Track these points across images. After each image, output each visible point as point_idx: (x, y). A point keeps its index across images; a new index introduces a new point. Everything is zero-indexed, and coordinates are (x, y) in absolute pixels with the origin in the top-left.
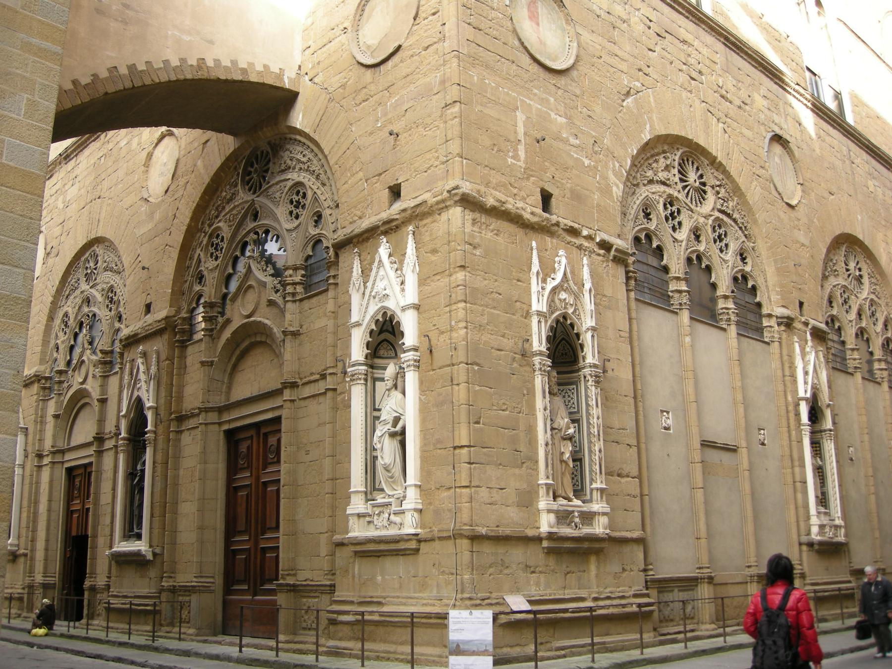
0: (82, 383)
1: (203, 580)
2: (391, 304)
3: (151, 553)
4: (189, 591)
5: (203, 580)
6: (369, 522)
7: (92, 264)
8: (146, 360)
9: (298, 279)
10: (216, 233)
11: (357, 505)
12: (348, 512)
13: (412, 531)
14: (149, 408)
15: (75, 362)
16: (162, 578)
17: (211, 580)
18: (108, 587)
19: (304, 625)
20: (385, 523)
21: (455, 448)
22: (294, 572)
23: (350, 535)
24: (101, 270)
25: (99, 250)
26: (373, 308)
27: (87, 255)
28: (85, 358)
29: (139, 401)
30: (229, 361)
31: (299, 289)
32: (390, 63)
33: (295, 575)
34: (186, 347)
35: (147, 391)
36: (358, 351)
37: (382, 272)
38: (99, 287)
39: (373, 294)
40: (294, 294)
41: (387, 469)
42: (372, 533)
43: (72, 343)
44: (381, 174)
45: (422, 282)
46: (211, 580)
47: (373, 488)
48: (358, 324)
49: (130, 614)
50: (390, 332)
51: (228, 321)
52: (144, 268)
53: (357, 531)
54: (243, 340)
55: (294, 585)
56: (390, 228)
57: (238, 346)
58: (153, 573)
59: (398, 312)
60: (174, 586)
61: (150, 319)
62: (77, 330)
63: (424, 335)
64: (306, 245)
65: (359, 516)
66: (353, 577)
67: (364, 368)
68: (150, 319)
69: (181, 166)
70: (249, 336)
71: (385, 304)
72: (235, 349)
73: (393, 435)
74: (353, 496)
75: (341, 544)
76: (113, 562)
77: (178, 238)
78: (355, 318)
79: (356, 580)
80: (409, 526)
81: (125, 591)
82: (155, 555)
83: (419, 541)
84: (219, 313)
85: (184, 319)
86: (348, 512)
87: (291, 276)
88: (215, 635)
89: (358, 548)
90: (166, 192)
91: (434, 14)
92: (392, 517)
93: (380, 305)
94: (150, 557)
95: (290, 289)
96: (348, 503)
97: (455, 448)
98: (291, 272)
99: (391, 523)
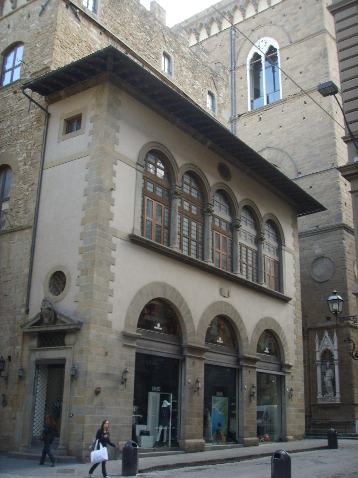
2: (329, 348)
11: (320, 396)
13: (339, 403)
20: (330, 400)
21: (350, 384)
23: (318, 403)
26: (323, 348)
32: (325, 283)
36: (318, 358)
37: (326, 340)
39: (324, 344)
41: (329, 387)
42: (325, 403)
44: (324, 313)
45: (339, 343)
47: (324, 392)
53: (320, 402)
56: (328, 328)
59: (333, 351)
63: (339, 356)
65: (321, 398)
67: (320, 362)
71: (328, 347)
73: (330, 380)
75: (314, 405)
78: (317, 350)
80: (338, 401)
91: (339, 274)
93: (325, 348)
96: (317, 395)
97: (350, 384)
99: (331, 400)
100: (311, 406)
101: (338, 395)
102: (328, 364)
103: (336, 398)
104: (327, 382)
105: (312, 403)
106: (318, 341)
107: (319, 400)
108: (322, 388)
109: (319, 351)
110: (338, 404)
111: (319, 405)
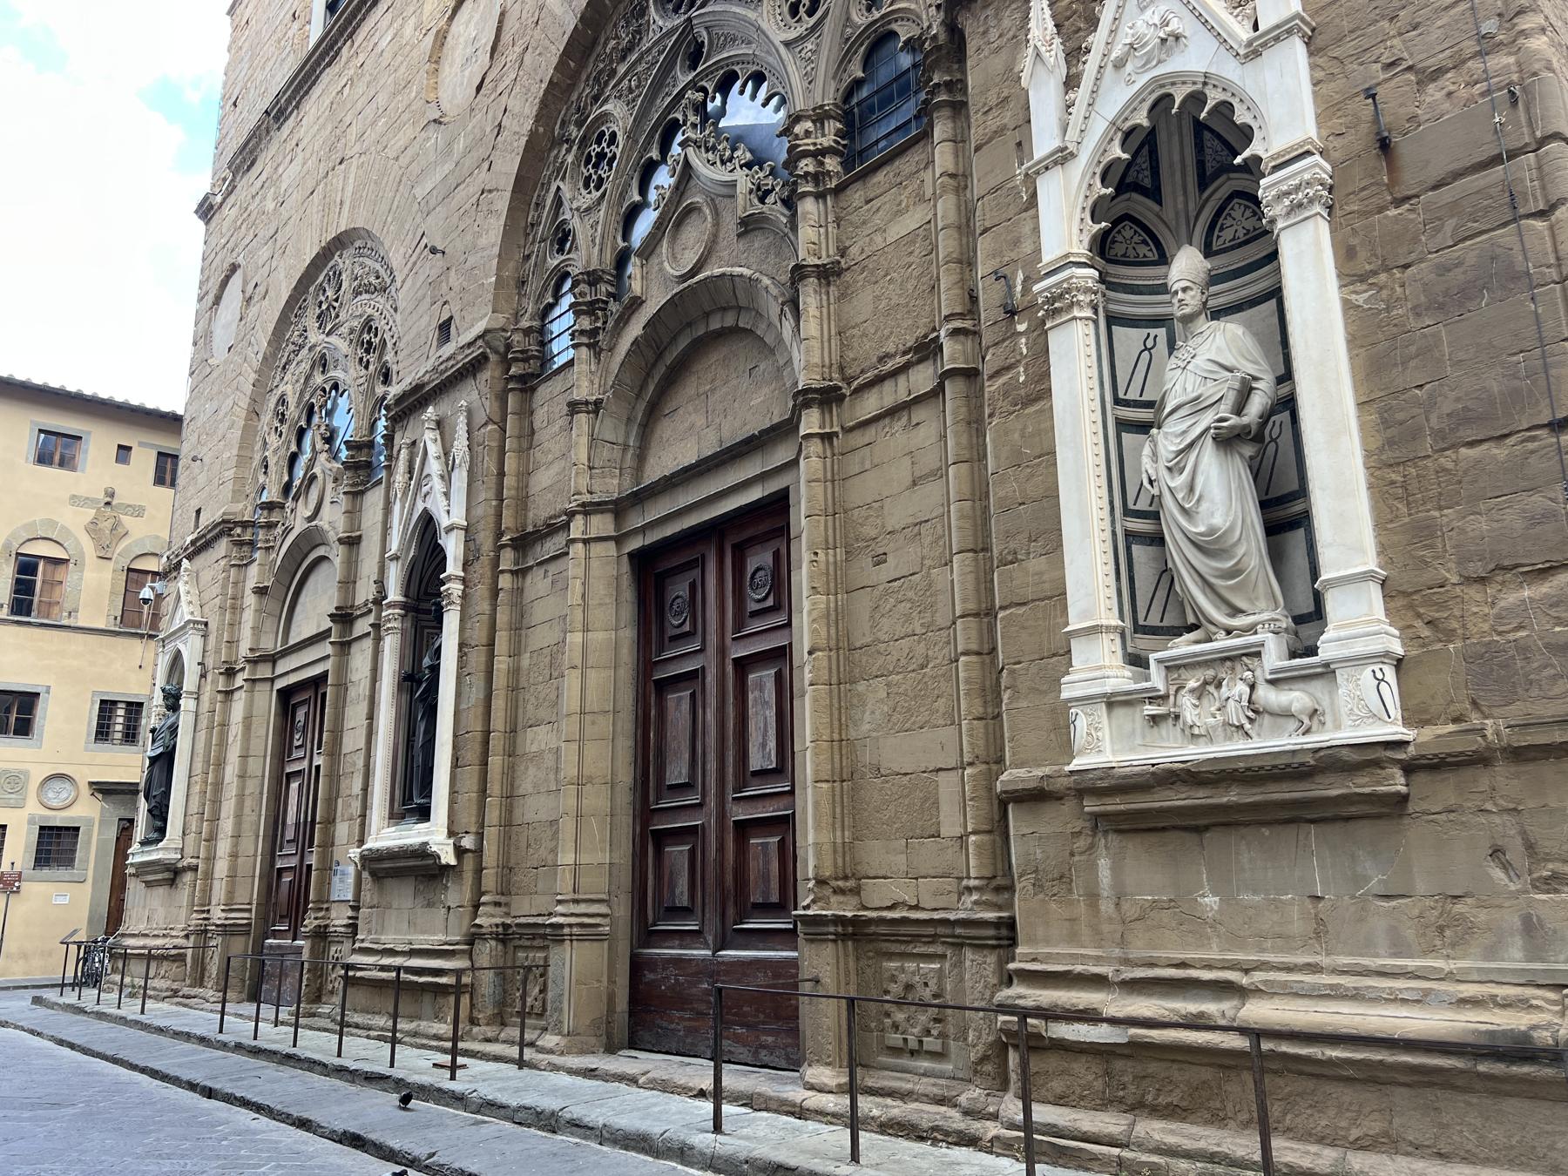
0: (310, 519)
1: (582, 908)
3: (451, 849)
4: (544, 937)
5: (582, 908)
6: (1155, 720)
7: (330, 293)
8: (442, 434)
9: (827, 141)
10: (597, 133)
12: (1065, 695)
14: (450, 529)
15: (297, 483)
16: (476, 906)
17: (603, 909)
18: (353, 928)
19: (895, 1039)
20: (1235, 713)
22: (851, 883)
23: (1077, 763)
24: (349, 296)
25: (344, 262)
27: (321, 278)
28: (317, 470)
29: (428, 521)
30: (638, 396)
31: (831, 163)
33: (856, 891)
34: (533, 389)
35: (447, 495)
36: (1063, 223)
38: (344, 330)
39: (1116, 52)
40: (816, 178)
41: (1210, 546)
42: (1171, 750)
43: (294, 448)
46: (603, 909)
47: (1157, 611)
48: (1063, 157)
49: (402, 993)
50: (1144, 192)
51: (637, 303)
52: (434, 251)
53: (1105, 746)
54: (674, 339)
55: (855, 921)
57: (660, 356)
58: (457, 894)
59: (1230, 70)
60: (506, 926)
61: (449, 349)
62: (303, 423)
64: (845, 59)
65: (1113, 702)
66: (1093, 897)
68: (449, 349)
69: (511, 26)
70: (689, 325)
72: (654, 365)
73: (1227, 440)
74: (1076, 646)
75: (1036, 797)
76: (365, 875)
77: (508, 165)
78: (1044, 142)
79: (1106, 907)
80: (1363, 710)
81: (389, 939)
82: (460, 852)
83: (1409, 769)
84: (609, 295)
85: (527, 332)
86: (1065, 695)
87: (807, 134)
88: (611, 1049)
89: (1116, 805)
90: (479, 88)
92: (1267, 695)
94: (448, 858)
95: (807, 165)
98: (809, 125)
99: (1256, 711)
100: (1005, 801)
101: (1359, 621)
102: (1187, 265)
103: (1327, 672)
104: (1179, 481)
105: (1014, 776)
106: (1055, 54)
107: (1082, 723)
108: (1125, 571)
109: (1063, 157)
110: (1371, 756)
111: (1090, 786)
